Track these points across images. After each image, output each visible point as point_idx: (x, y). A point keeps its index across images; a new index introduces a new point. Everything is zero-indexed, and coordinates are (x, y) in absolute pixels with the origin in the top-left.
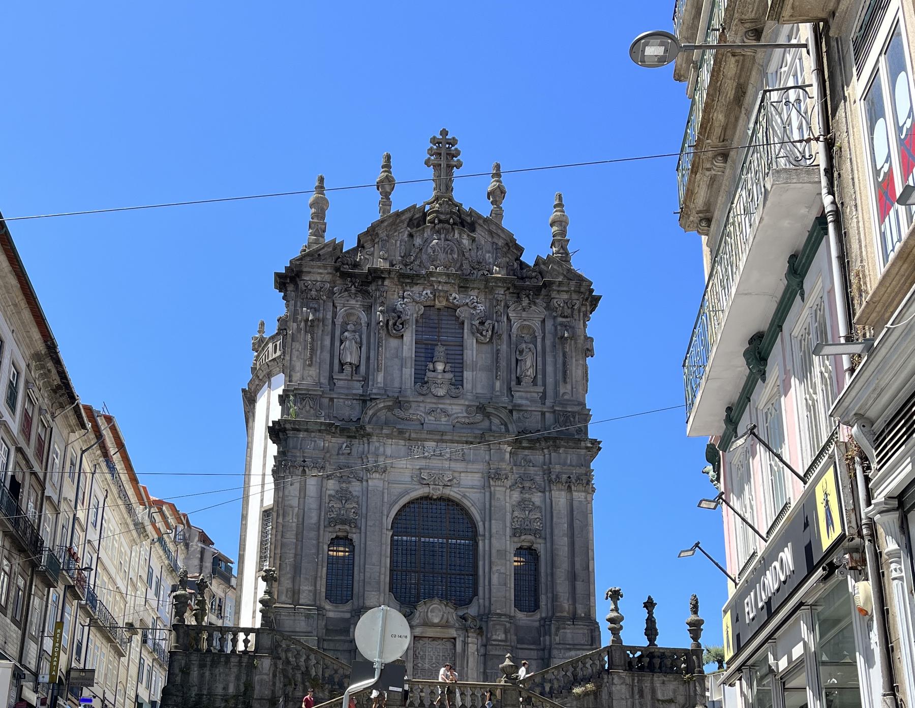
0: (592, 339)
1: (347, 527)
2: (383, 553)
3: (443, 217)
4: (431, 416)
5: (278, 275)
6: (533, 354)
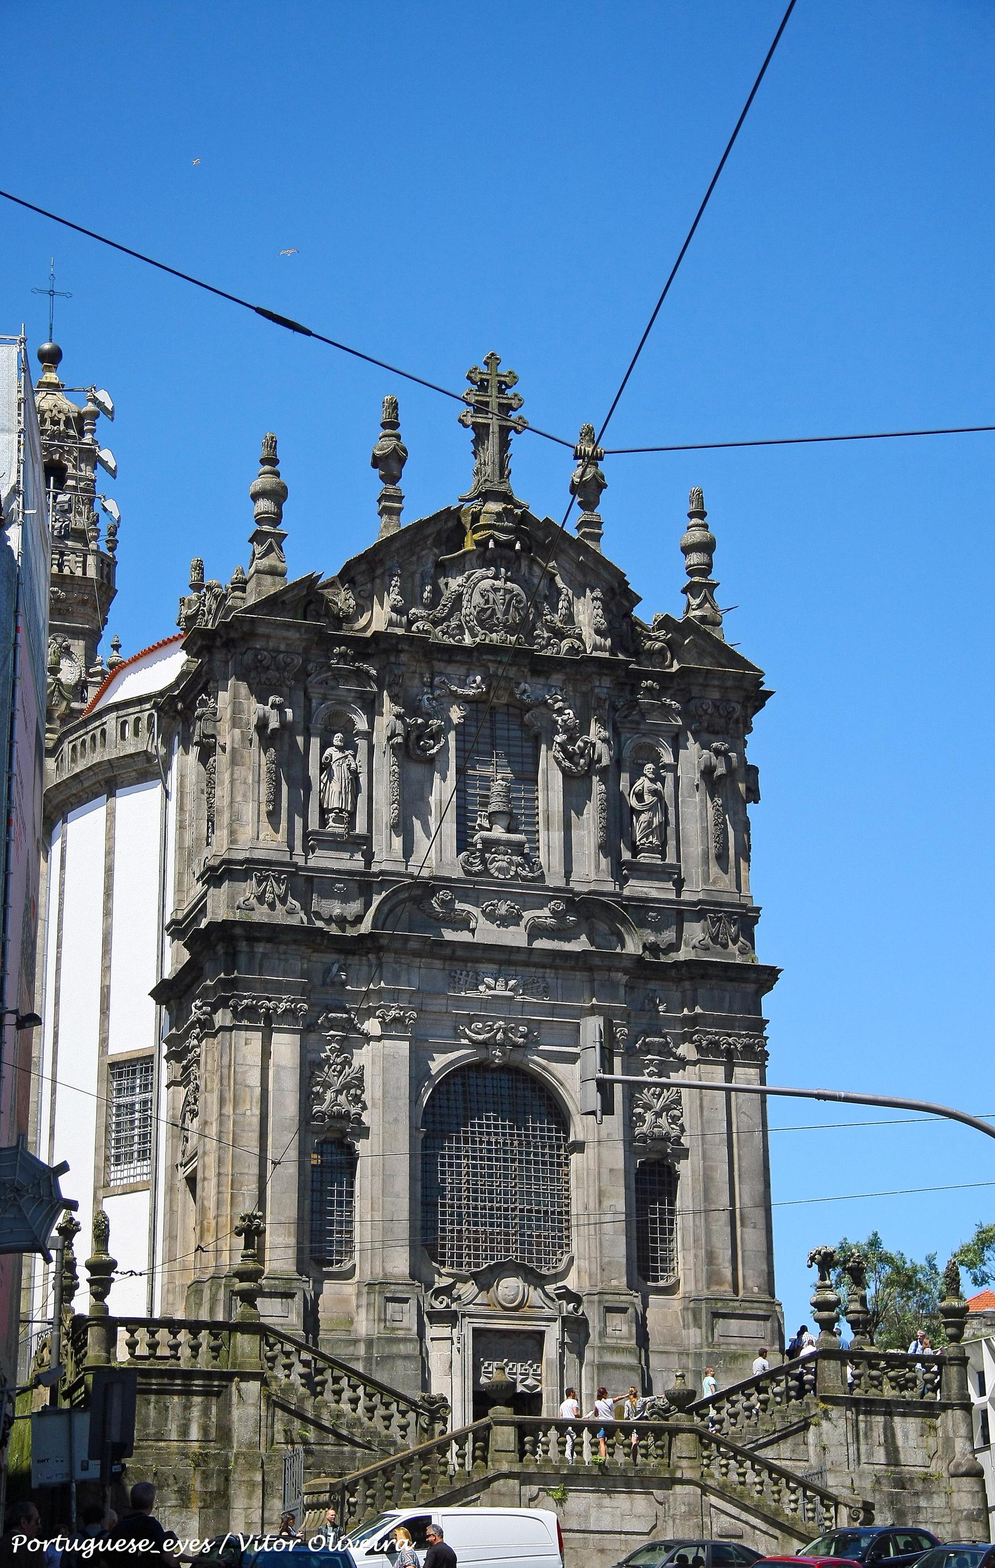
0: (755, 770)
3: (503, 537)
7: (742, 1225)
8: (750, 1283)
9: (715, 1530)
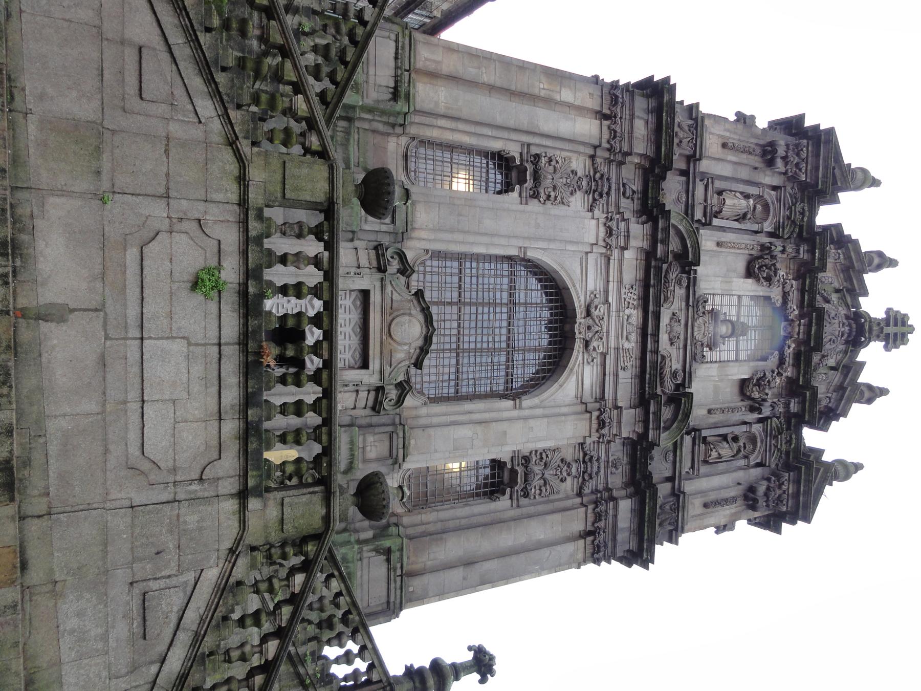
1: (529, 183)
2: (496, 240)
3: (867, 328)
4: (671, 319)
5: (801, 118)
6: (732, 456)
9: (154, 585)
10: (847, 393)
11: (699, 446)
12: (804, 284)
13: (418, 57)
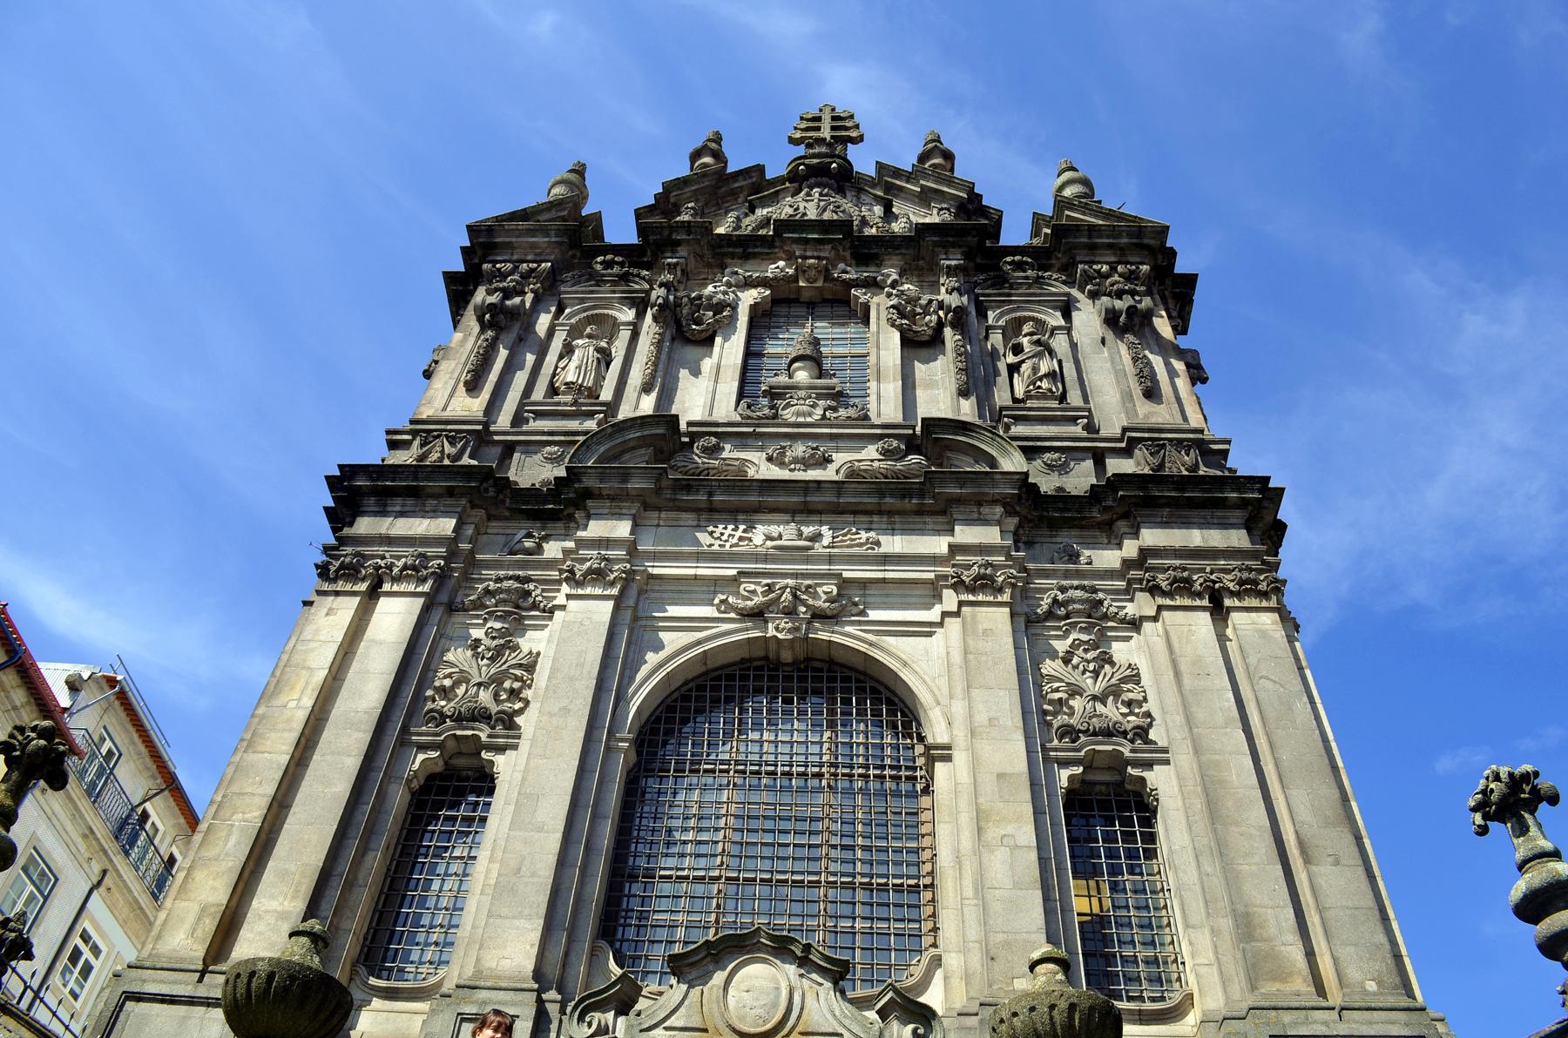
5: (450, 278)
7: (1307, 860)
8: (1353, 974)
10: (930, 184)
11: (1030, 409)
12: (733, 256)
13: (183, 953)
